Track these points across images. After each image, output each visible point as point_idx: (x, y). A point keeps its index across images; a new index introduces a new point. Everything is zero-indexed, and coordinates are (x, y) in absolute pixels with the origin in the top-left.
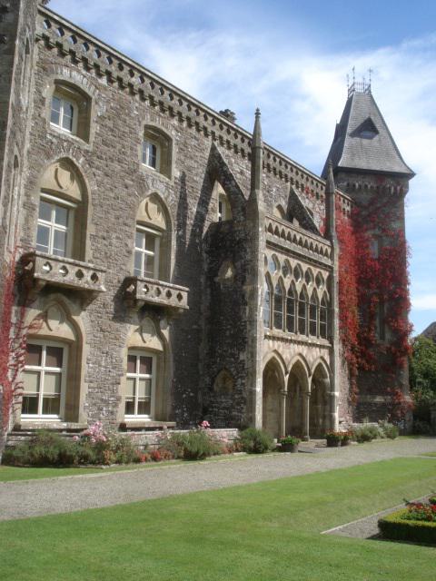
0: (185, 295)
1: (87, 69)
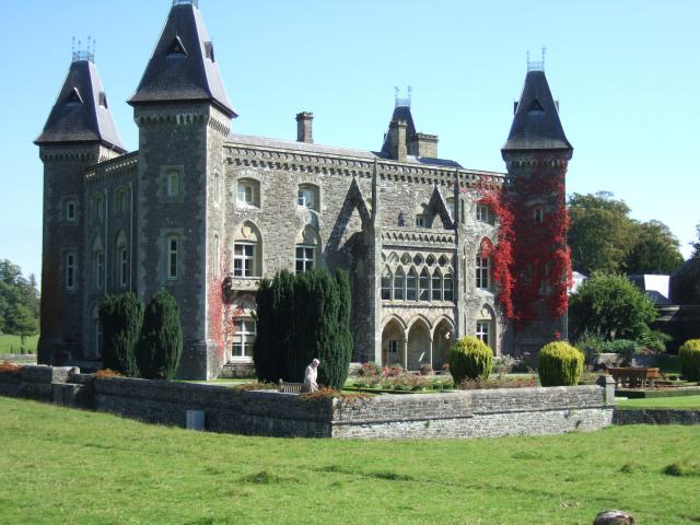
1: (255, 165)
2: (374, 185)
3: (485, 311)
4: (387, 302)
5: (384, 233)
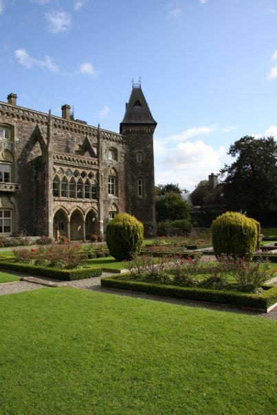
0: (20, 187)
2: (48, 129)
3: (113, 207)
4: (57, 198)
5: (55, 156)
